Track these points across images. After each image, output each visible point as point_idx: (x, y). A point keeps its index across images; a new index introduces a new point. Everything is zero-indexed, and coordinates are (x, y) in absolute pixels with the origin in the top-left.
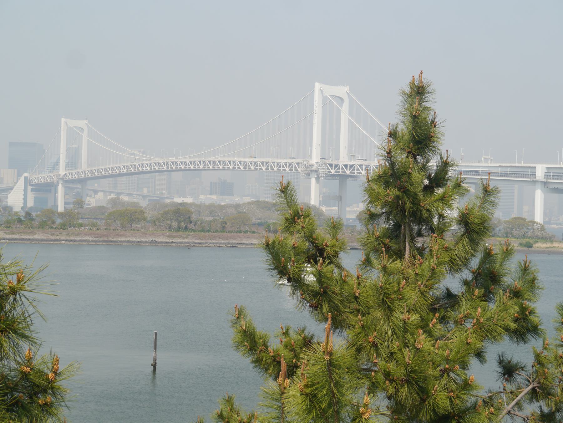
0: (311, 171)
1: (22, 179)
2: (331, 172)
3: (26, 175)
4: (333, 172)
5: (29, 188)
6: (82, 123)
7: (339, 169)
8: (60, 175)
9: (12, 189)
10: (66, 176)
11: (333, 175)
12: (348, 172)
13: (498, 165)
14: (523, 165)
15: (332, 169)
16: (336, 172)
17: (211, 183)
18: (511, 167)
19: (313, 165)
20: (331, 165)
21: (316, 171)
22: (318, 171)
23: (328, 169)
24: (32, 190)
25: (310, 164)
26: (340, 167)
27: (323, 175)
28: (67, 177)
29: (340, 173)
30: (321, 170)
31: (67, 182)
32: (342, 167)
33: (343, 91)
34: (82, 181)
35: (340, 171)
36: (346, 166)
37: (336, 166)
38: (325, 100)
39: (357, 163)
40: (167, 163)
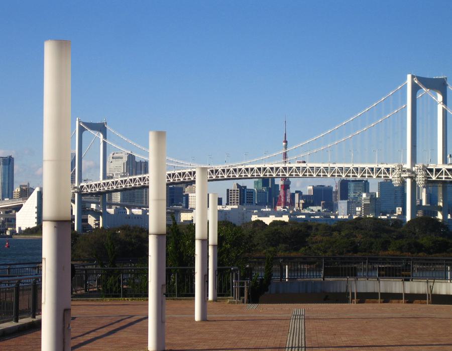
0: (406, 177)
2: (431, 178)
4: (434, 178)
7: (442, 174)
8: (75, 188)
10: (84, 189)
11: (434, 181)
15: (432, 174)
16: (438, 178)
17: (228, 190)
19: (409, 171)
20: (431, 170)
22: (416, 176)
23: (428, 174)
25: (406, 169)
26: (442, 172)
27: (421, 182)
28: (85, 190)
29: (444, 179)
30: (418, 176)
32: (445, 172)
35: (444, 176)
40: (217, 171)
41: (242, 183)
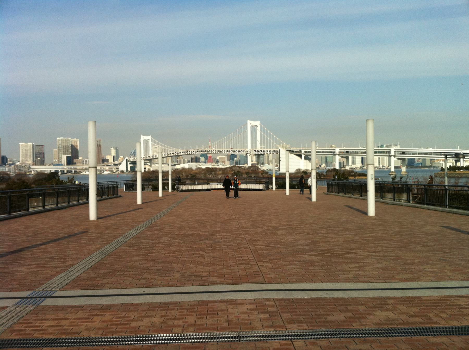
1: (125, 160)
3: (127, 158)
4: (256, 153)
5: (128, 163)
6: (149, 138)
7: (258, 152)
9: (120, 164)
12: (262, 153)
13: (321, 149)
14: (330, 149)
18: (326, 149)
20: (255, 151)
21: (249, 153)
24: (129, 164)
31: (144, 160)
33: (257, 123)
34: (150, 160)
36: (261, 151)
37: (257, 151)
38: (252, 127)
39: (266, 150)
41: (196, 156)
